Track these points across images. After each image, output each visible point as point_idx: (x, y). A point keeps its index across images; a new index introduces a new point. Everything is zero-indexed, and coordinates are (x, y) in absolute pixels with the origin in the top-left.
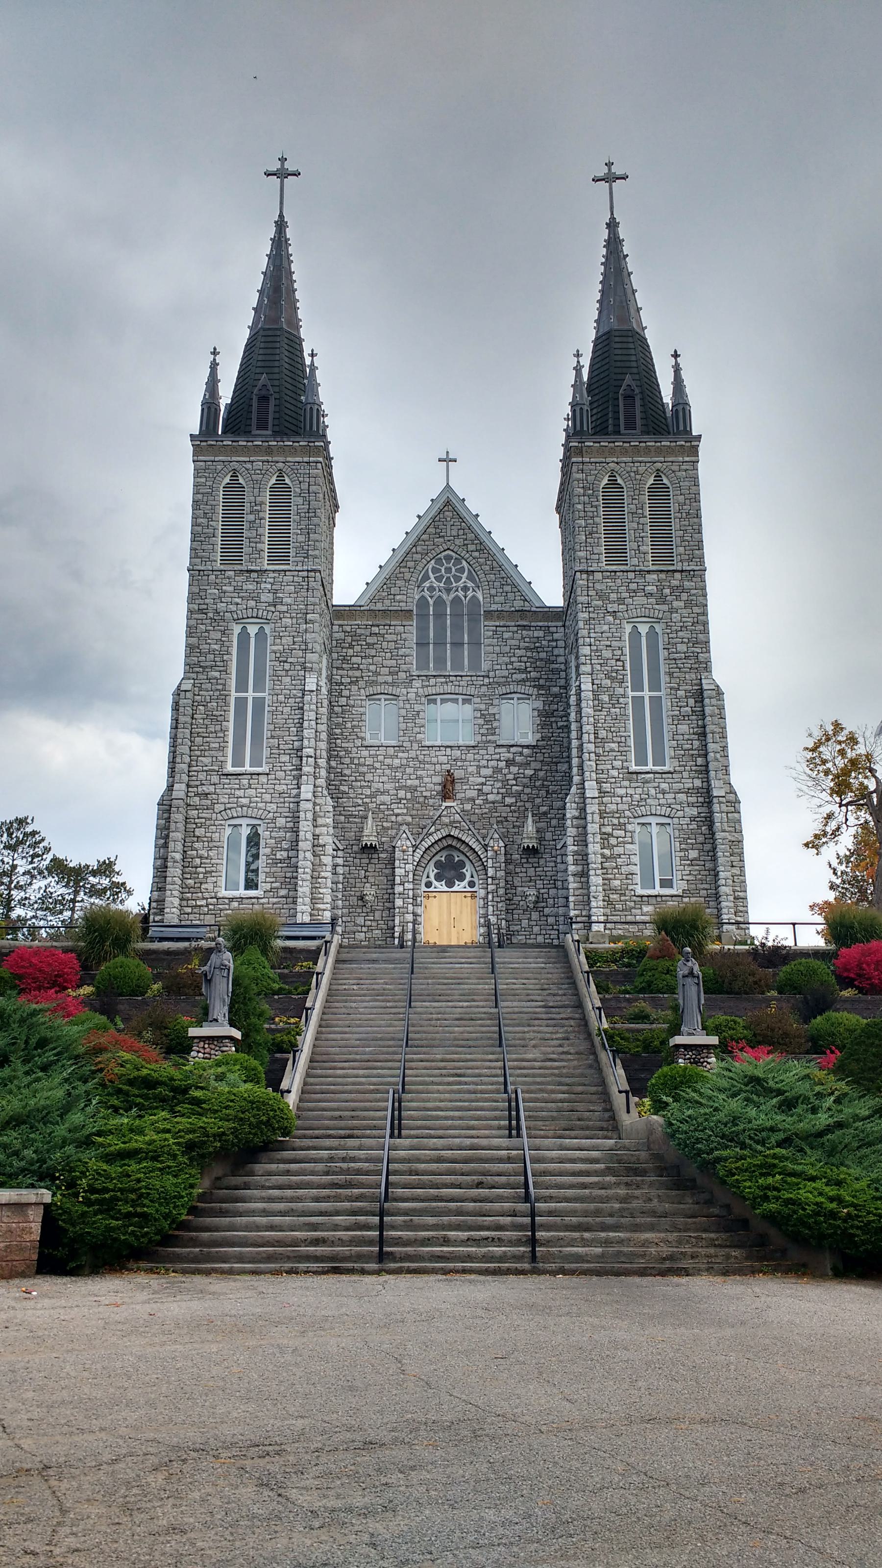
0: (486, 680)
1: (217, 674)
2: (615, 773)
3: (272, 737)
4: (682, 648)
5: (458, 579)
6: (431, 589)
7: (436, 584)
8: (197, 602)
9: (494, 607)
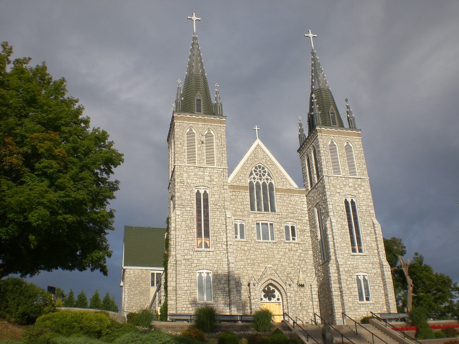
0: (279, 216)
1: (189, 209)
2: (346, 255)
3: (214, 236)
4: (364, 208)
5: (264, 175)
6: (254, 178)
7: (256, 176)
8: (180, 178)
9: (279, 187)
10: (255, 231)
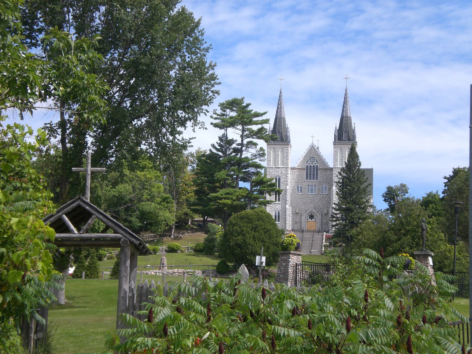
5: (314, 161)
6: (309, 164)
10: (307, 189)
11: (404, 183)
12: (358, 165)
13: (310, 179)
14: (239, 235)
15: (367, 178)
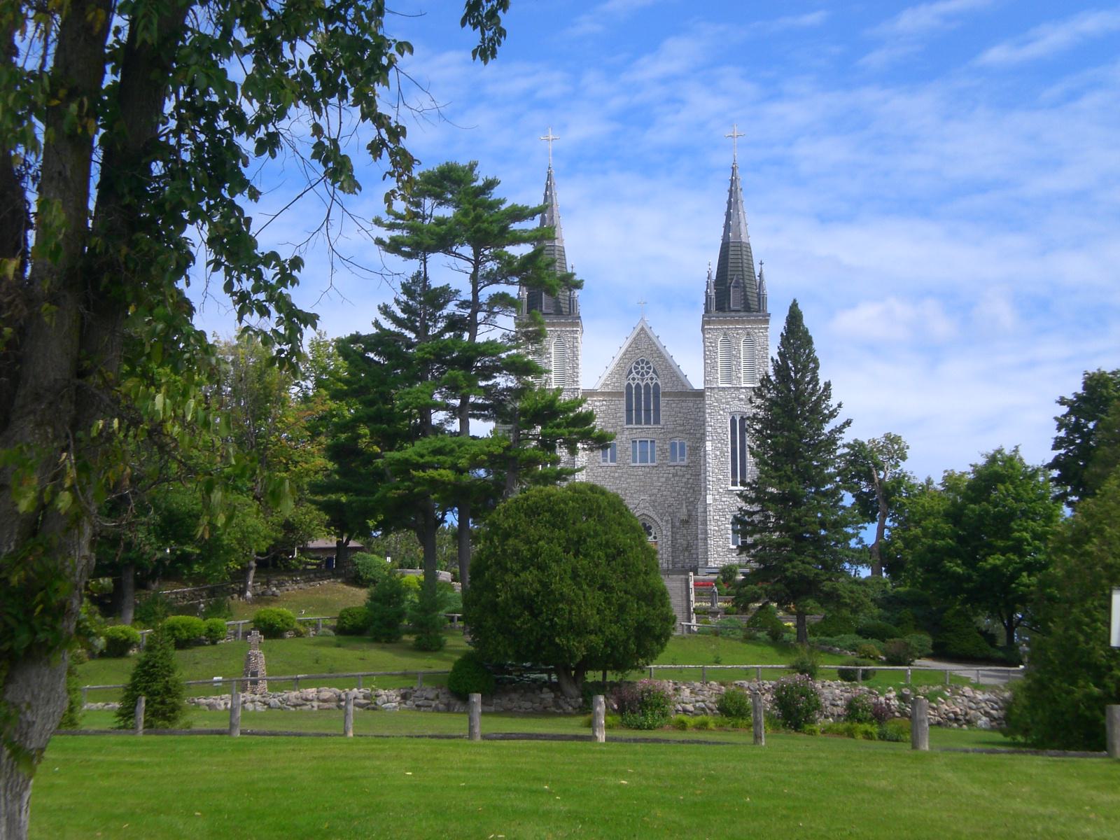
5: (648, 373)
6: (634, 379)
7: (636, 376)
10: (630, 452)
11: (895, 432)
12: (812, 365)
13: (638, 422)
14: (524, 568)
15: (840, 406)
